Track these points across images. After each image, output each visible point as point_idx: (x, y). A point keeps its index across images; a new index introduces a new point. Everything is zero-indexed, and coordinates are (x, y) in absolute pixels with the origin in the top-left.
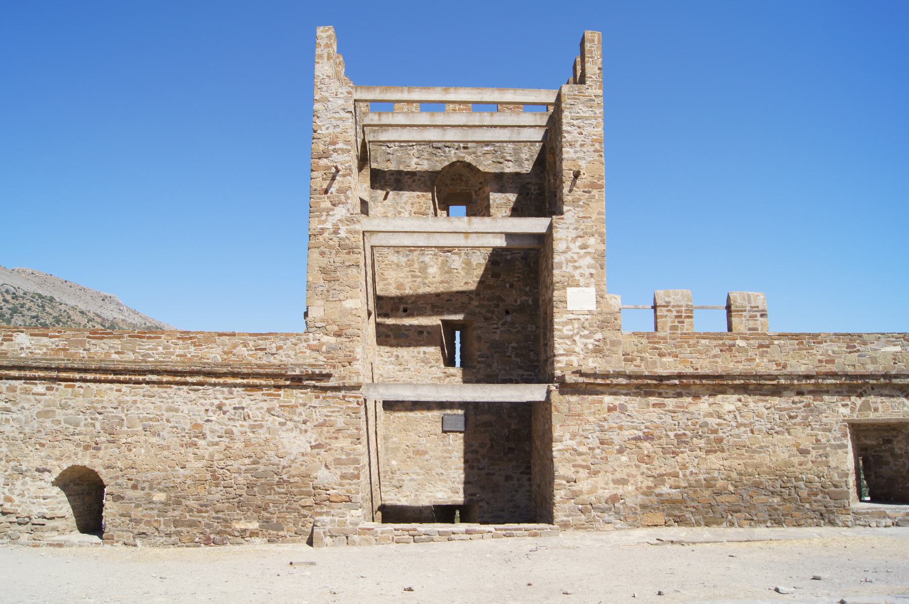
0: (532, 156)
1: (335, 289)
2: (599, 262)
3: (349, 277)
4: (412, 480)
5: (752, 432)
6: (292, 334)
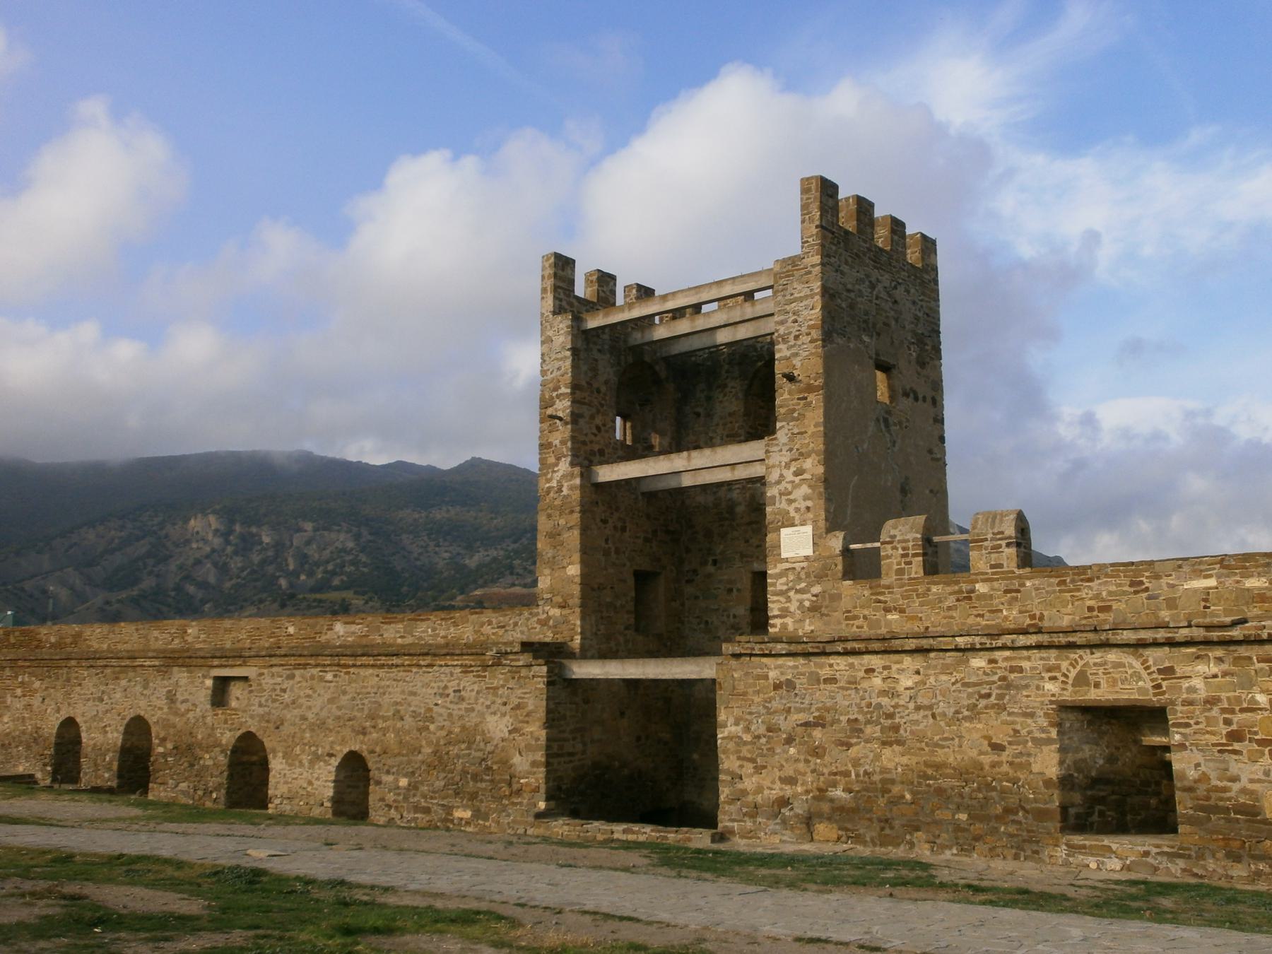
5: (934, 716)
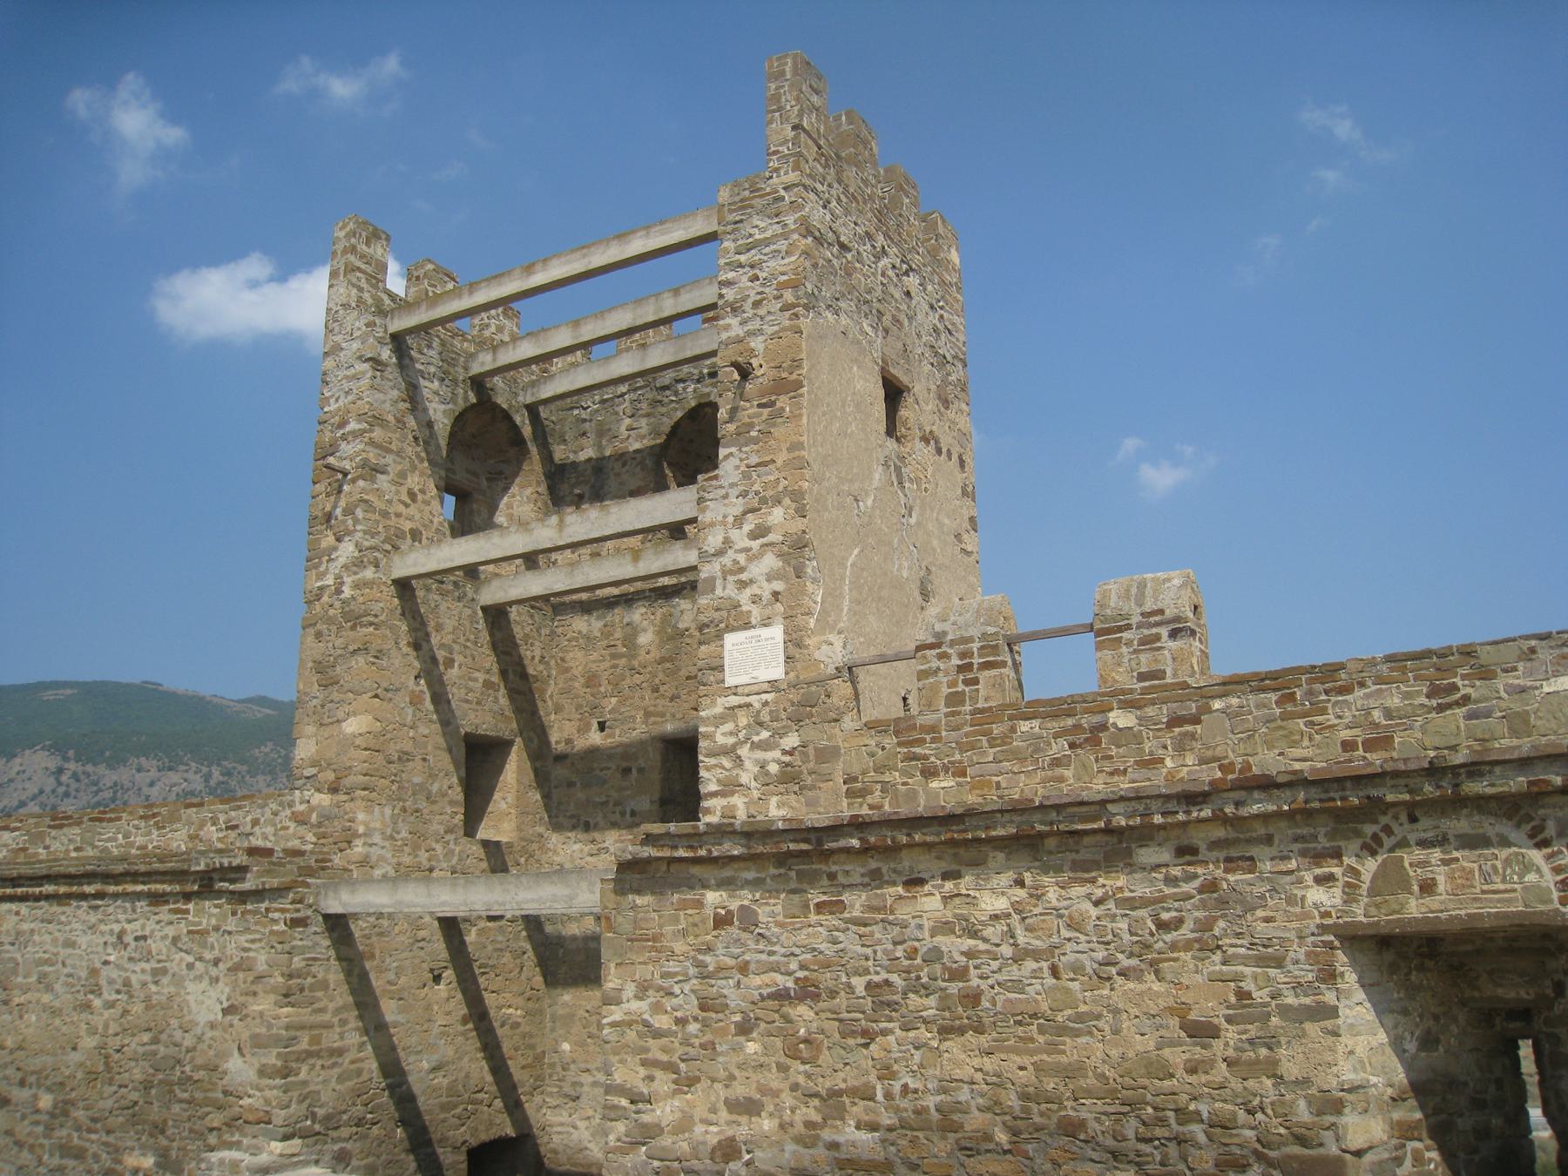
2: (793, 562)
5: (1055, 972)
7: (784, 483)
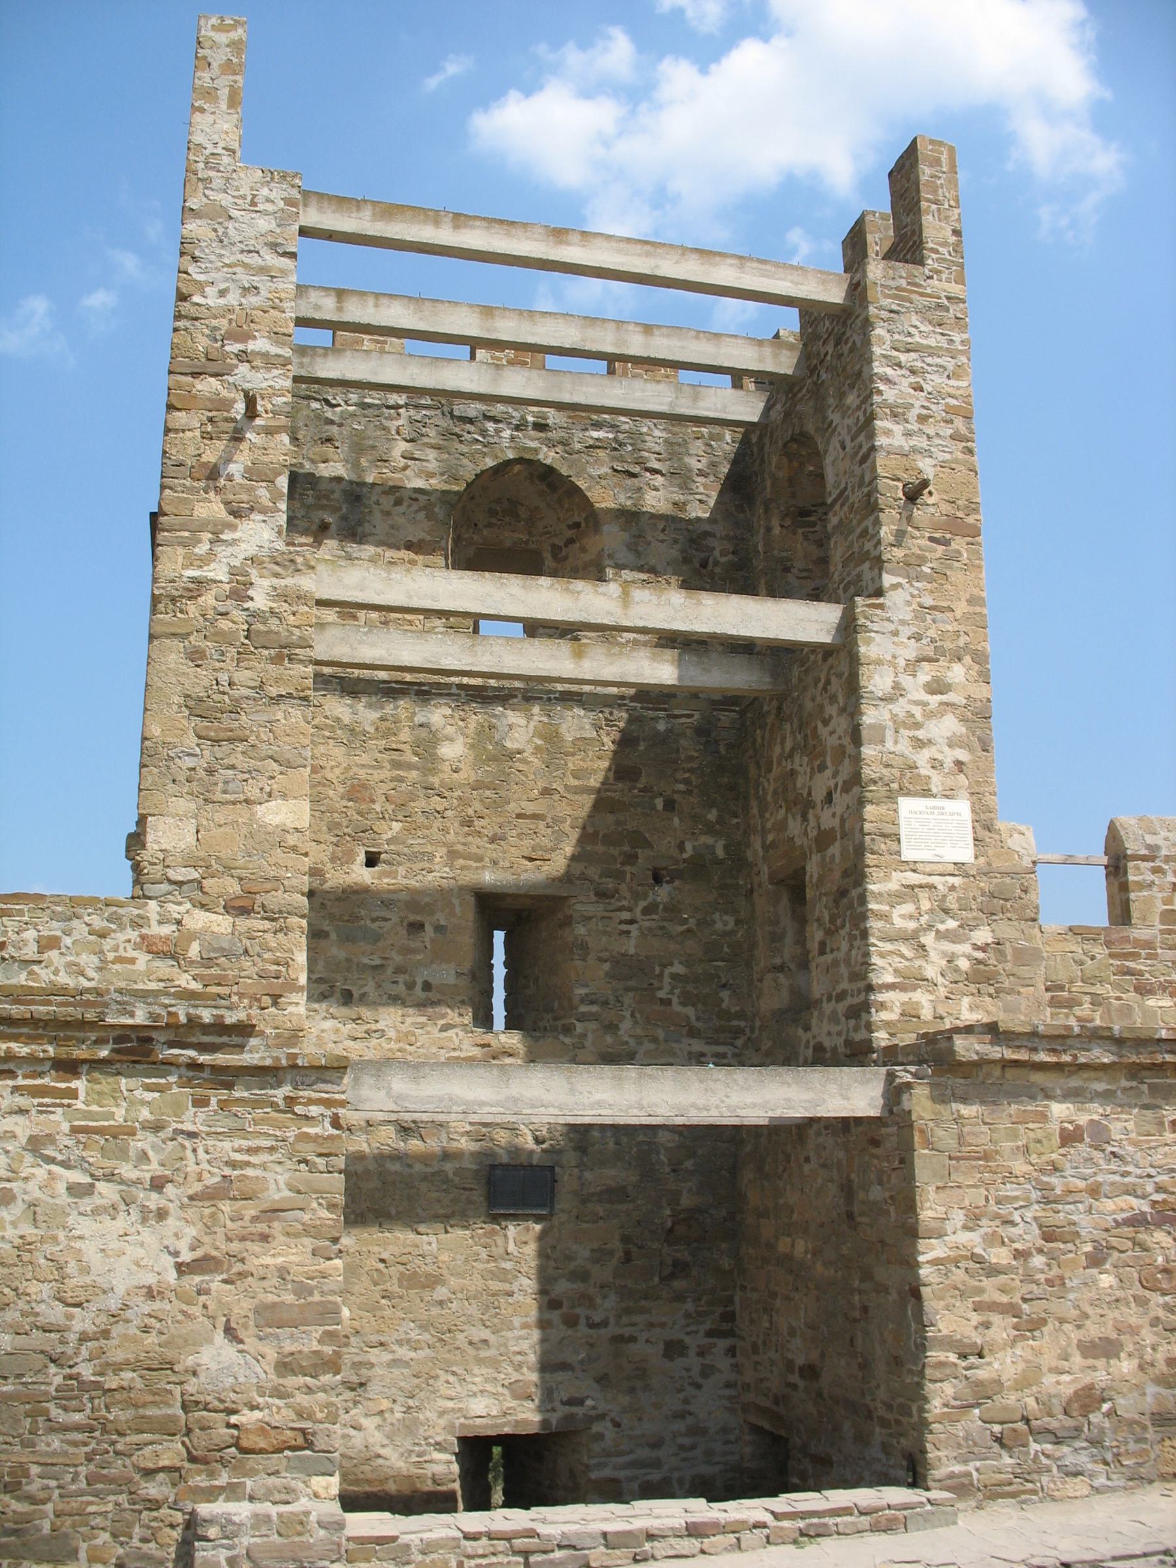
0: (713, 465)
1: (233, 767)
3: (278, 732)
4: (395, 1363)
6: (92, 902)
7: (963, 640)
